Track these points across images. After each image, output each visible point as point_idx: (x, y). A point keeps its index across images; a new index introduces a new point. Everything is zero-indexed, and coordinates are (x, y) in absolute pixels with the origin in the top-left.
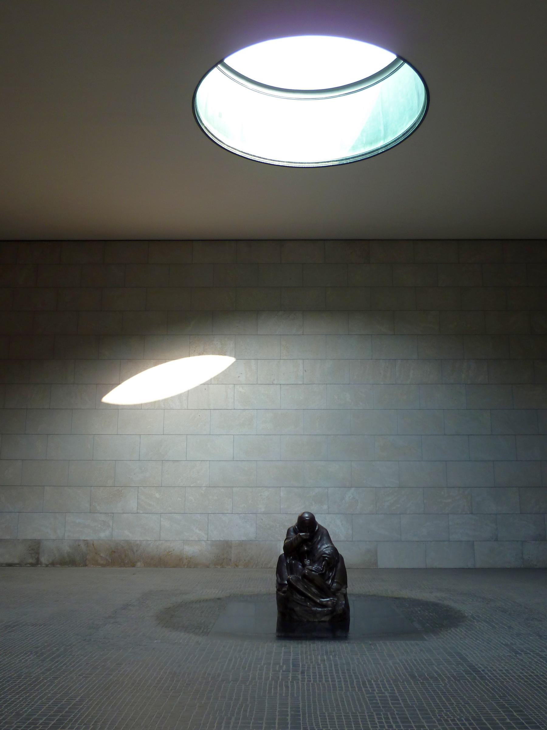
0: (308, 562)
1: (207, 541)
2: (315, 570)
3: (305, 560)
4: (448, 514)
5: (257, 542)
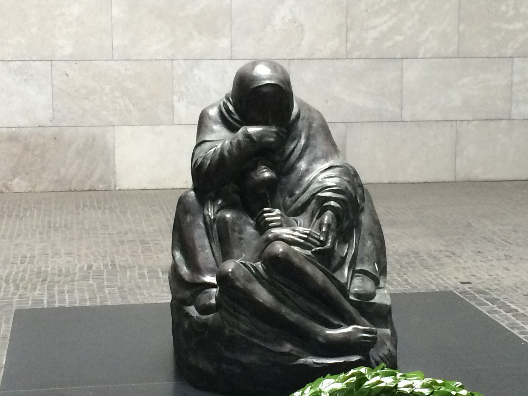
2: (302, 241)
3: (266, 209)
4: (513, 57)
5: (57, 128)
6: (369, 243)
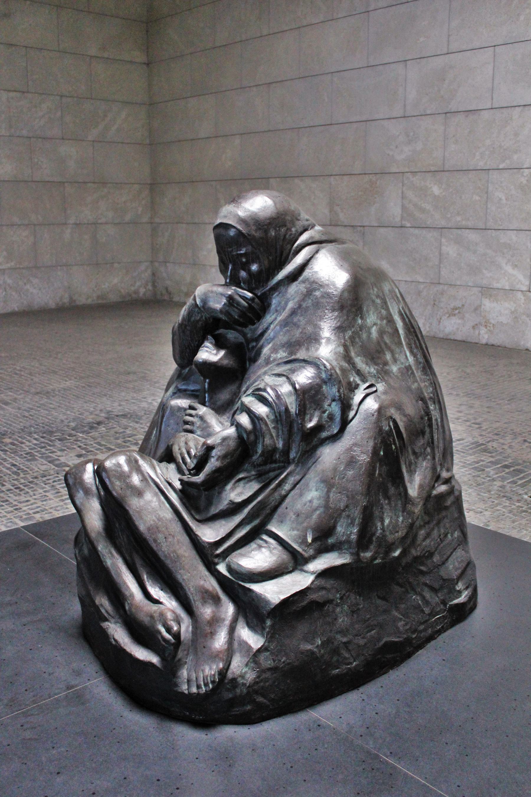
1: (528, 293)
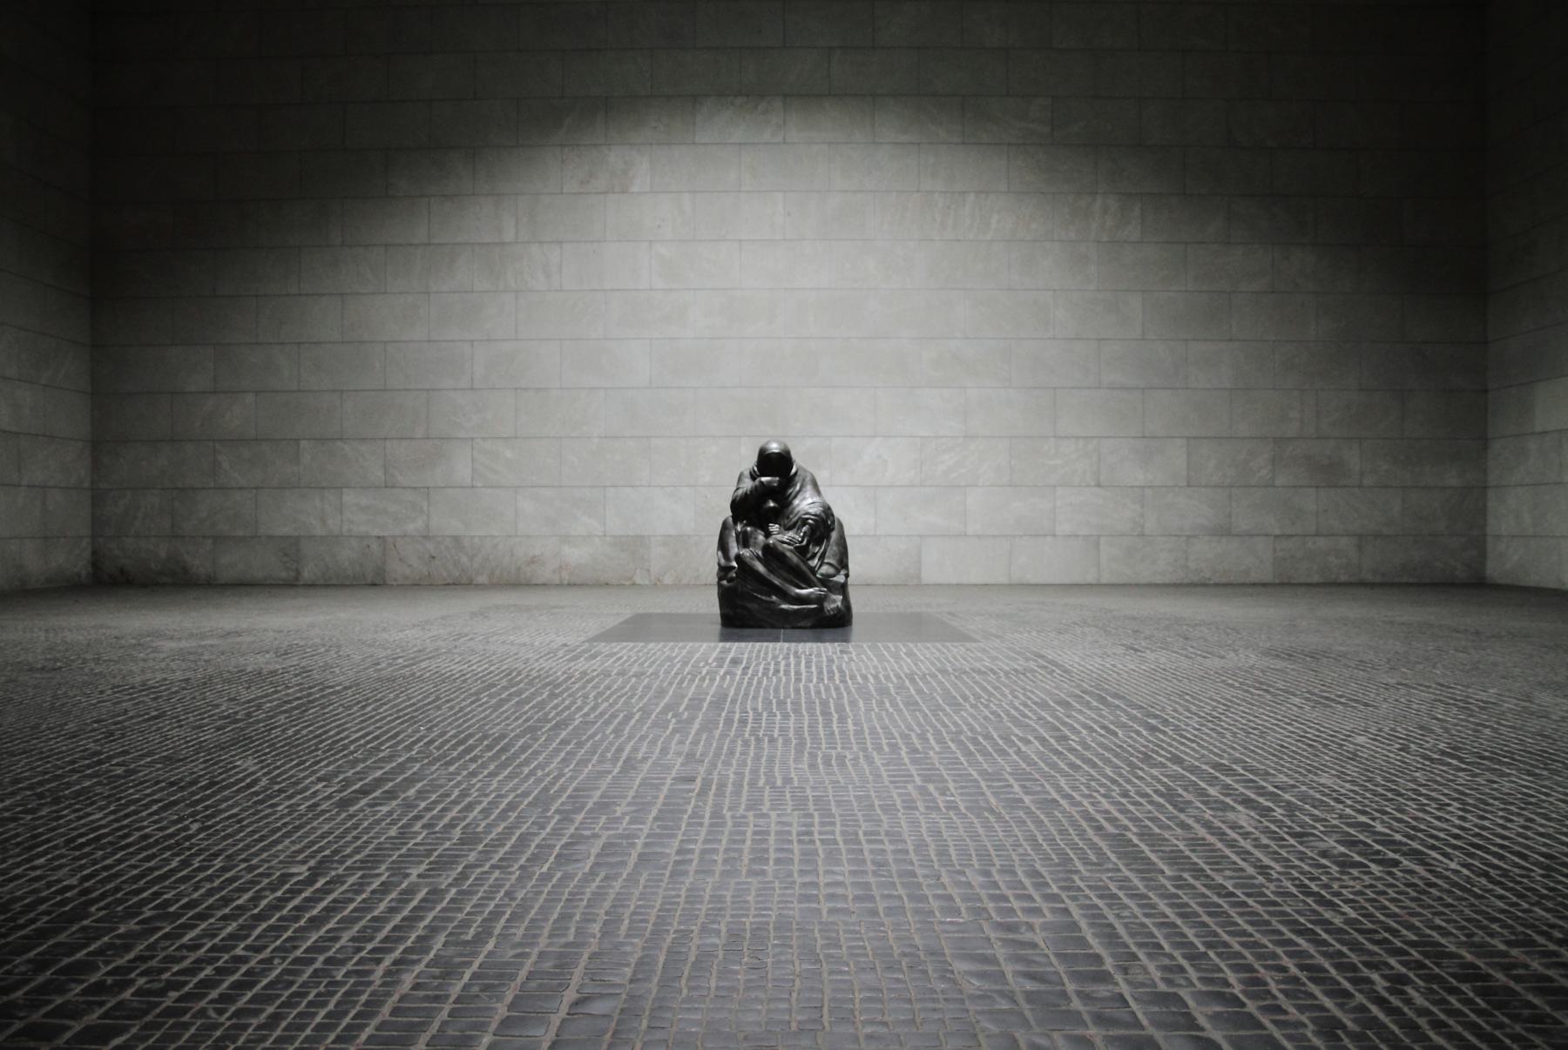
0: (774, 528)
4: (1055, 486)
6: (835, 548)
